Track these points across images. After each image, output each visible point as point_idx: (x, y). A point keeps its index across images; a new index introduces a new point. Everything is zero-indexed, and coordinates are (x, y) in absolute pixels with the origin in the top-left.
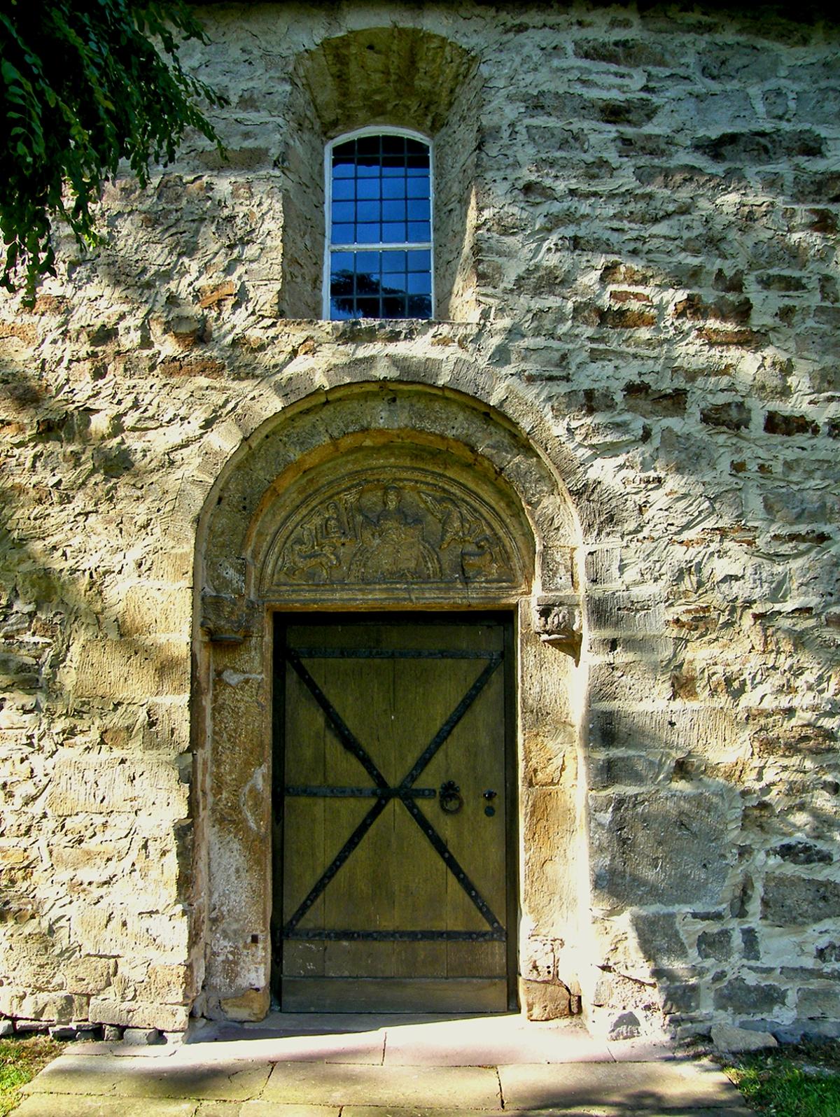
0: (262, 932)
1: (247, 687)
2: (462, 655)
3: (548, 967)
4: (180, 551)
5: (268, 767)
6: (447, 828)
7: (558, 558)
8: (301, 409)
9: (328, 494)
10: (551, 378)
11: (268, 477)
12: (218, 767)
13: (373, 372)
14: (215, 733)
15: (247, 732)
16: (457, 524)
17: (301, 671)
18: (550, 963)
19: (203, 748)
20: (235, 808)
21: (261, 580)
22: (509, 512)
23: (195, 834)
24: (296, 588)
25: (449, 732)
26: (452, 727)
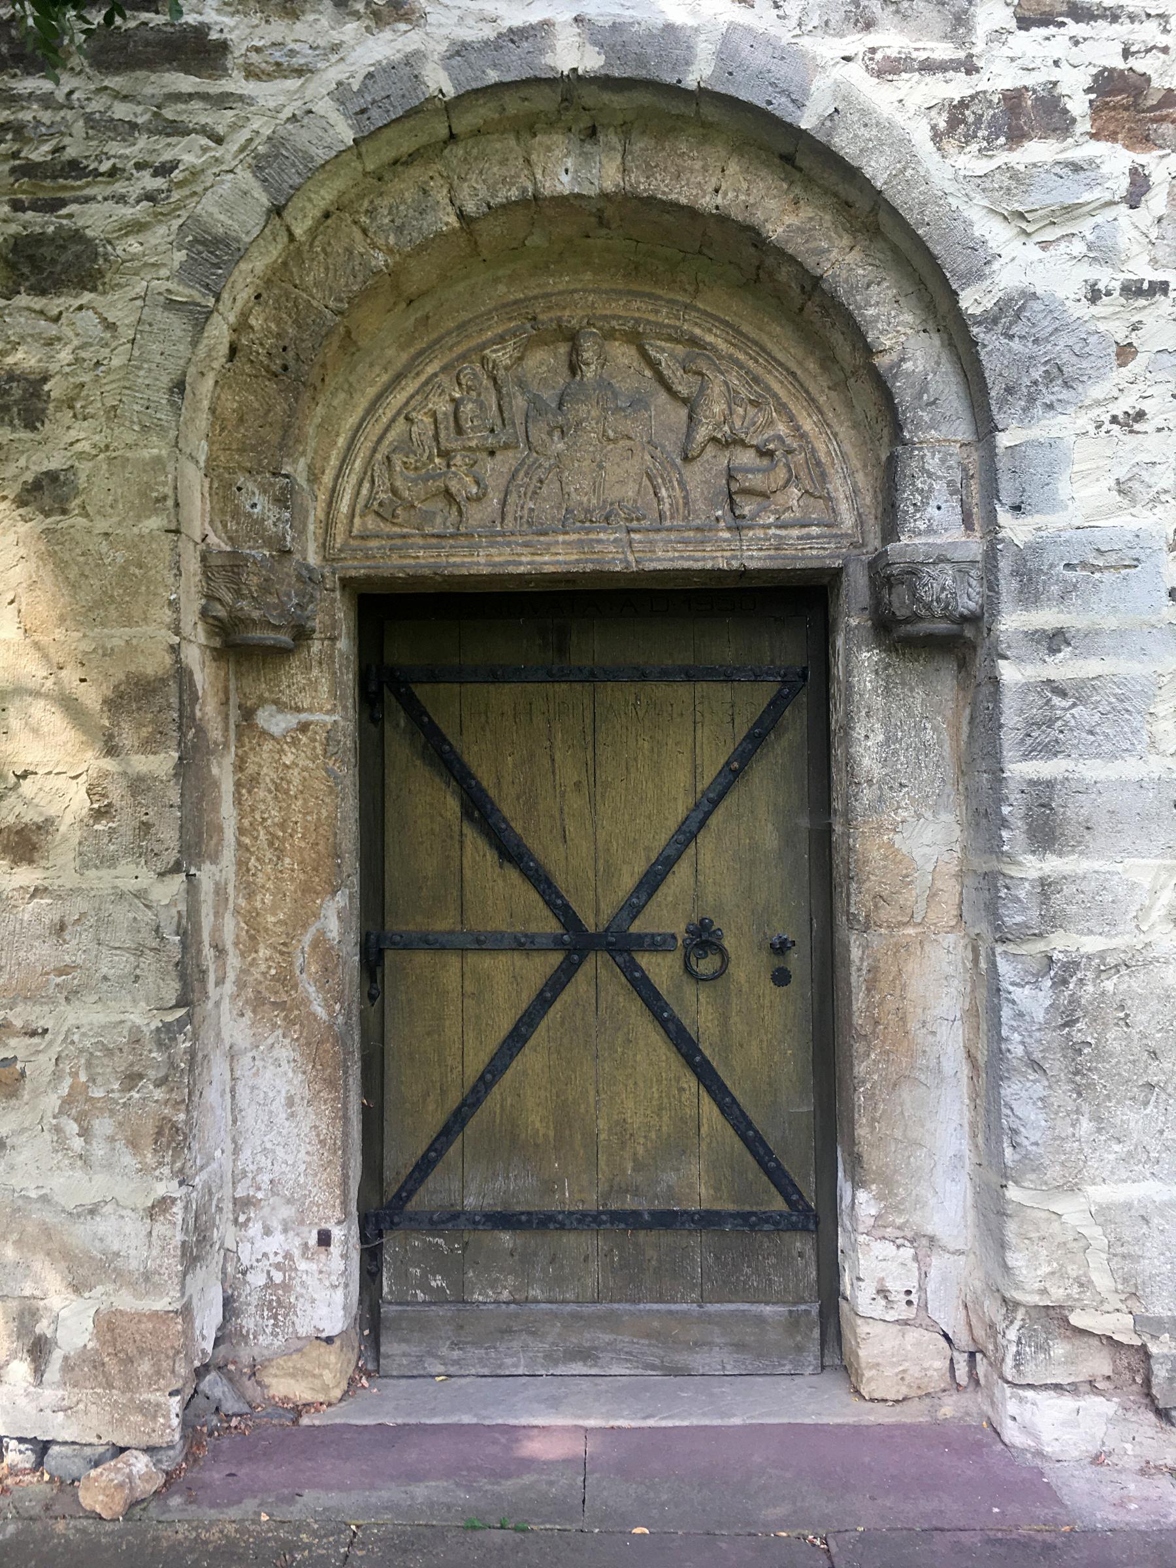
0: (339, 1223)
2: (727, 676)
3: (908, 1292)
4: (146, 454)
5: (351, 897)
6: (700, 1012)
7: (933, 462)
8: (393, 154)
9: (458, 350)
10: (929, 67)
11: (331, 304)
12: (250, 897)
13: (548, 59)
14: (241, 831)
15: (305, 828)
17: (415, 711)
18: (913, 1284)
19: (215, 858)
20: (285, 979)
21: (328, 525)
22: (824, 381)
23: (195, 1037)
24: (399, 542)
25: (702, 824)
26: (708, 815)
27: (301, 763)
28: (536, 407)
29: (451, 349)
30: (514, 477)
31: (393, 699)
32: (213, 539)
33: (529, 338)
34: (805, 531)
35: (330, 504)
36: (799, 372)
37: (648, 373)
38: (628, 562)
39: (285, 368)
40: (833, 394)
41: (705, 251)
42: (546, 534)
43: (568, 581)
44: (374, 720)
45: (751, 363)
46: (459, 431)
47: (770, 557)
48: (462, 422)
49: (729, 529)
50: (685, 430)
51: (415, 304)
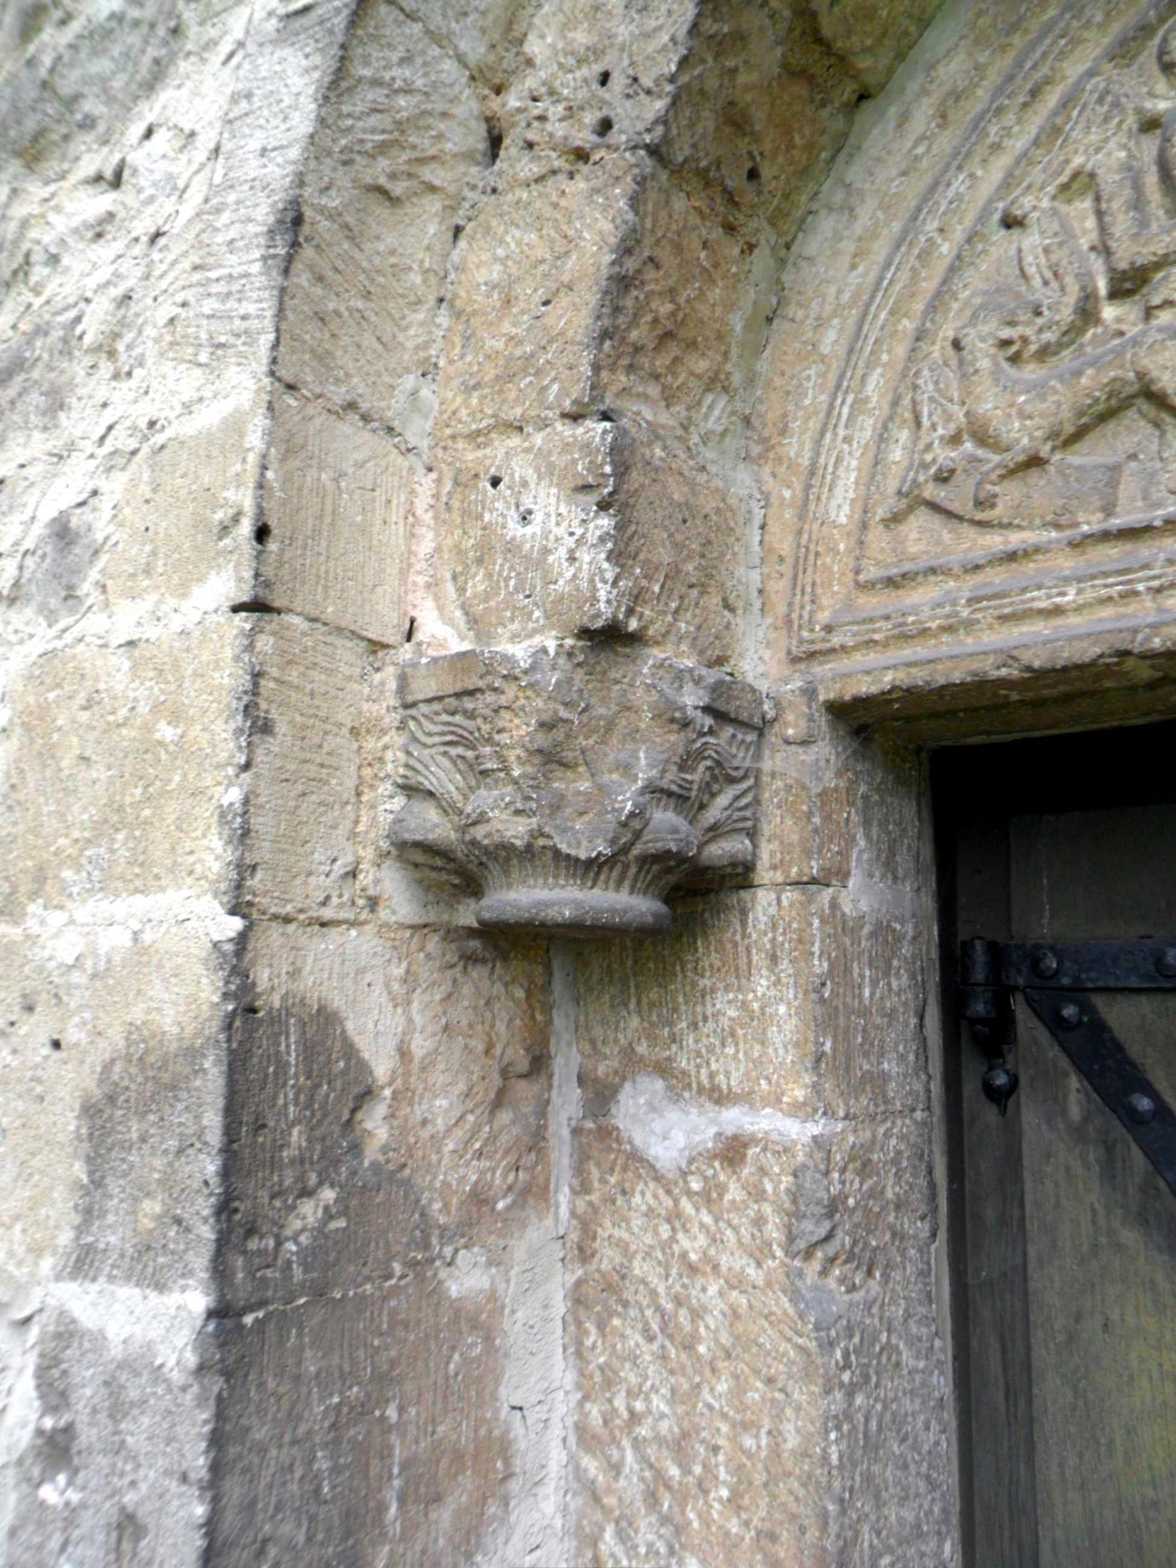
1: (734, 1192)
14: (585, 1437)
24: (996, 577)
27: (724, 1261)
31: (1043, 1035)
32: (431, 626)
35: (802, 513)
39: (605, 126)
44: (1000, 1097)
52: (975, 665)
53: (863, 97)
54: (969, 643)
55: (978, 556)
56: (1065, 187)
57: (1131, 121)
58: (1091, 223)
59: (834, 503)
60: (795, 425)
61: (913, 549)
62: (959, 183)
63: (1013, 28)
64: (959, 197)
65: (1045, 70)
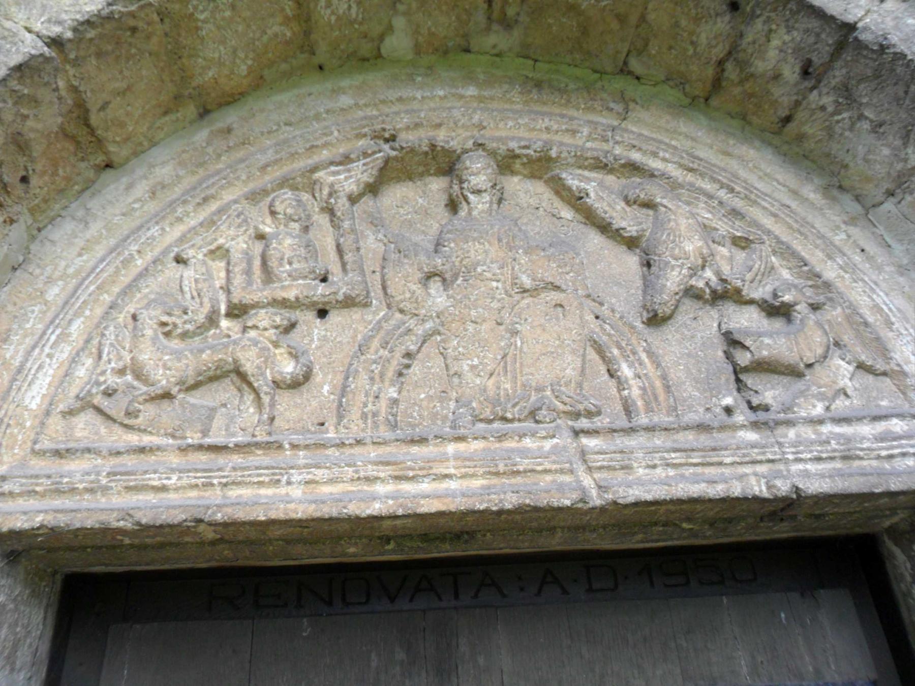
16: (692, 245)
24: (130, 461)
28: (399, 249)
29: (263, 168)
30: (362, 349)
33: (387, 160)
34: (880, 427)
36: (794, 205)
37: (567, 214)
38: (583, 490)
40: (854, 231)
41: (635, 65)
42: (423, 441)
43: (457, 537)
45: (722, 194)
46: (268, 275)
47: (840, 474)
48: (273, 263)
49: (755, 425)
50: (639, 283)
51: (215, 115)
52: (103, 517)
53: (108, 166)
54: (102, 501)
55: (121, 446)
56: (212, 252)
57: (251, 231)
58: (223, 274)
59: (30, 394)
60: (15, 338)
61: (79, 434)
62: (155, 231)
63: (201, 165)
64: (153, 238)
65: (212, 191)
